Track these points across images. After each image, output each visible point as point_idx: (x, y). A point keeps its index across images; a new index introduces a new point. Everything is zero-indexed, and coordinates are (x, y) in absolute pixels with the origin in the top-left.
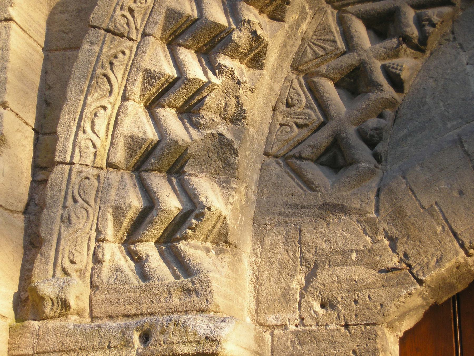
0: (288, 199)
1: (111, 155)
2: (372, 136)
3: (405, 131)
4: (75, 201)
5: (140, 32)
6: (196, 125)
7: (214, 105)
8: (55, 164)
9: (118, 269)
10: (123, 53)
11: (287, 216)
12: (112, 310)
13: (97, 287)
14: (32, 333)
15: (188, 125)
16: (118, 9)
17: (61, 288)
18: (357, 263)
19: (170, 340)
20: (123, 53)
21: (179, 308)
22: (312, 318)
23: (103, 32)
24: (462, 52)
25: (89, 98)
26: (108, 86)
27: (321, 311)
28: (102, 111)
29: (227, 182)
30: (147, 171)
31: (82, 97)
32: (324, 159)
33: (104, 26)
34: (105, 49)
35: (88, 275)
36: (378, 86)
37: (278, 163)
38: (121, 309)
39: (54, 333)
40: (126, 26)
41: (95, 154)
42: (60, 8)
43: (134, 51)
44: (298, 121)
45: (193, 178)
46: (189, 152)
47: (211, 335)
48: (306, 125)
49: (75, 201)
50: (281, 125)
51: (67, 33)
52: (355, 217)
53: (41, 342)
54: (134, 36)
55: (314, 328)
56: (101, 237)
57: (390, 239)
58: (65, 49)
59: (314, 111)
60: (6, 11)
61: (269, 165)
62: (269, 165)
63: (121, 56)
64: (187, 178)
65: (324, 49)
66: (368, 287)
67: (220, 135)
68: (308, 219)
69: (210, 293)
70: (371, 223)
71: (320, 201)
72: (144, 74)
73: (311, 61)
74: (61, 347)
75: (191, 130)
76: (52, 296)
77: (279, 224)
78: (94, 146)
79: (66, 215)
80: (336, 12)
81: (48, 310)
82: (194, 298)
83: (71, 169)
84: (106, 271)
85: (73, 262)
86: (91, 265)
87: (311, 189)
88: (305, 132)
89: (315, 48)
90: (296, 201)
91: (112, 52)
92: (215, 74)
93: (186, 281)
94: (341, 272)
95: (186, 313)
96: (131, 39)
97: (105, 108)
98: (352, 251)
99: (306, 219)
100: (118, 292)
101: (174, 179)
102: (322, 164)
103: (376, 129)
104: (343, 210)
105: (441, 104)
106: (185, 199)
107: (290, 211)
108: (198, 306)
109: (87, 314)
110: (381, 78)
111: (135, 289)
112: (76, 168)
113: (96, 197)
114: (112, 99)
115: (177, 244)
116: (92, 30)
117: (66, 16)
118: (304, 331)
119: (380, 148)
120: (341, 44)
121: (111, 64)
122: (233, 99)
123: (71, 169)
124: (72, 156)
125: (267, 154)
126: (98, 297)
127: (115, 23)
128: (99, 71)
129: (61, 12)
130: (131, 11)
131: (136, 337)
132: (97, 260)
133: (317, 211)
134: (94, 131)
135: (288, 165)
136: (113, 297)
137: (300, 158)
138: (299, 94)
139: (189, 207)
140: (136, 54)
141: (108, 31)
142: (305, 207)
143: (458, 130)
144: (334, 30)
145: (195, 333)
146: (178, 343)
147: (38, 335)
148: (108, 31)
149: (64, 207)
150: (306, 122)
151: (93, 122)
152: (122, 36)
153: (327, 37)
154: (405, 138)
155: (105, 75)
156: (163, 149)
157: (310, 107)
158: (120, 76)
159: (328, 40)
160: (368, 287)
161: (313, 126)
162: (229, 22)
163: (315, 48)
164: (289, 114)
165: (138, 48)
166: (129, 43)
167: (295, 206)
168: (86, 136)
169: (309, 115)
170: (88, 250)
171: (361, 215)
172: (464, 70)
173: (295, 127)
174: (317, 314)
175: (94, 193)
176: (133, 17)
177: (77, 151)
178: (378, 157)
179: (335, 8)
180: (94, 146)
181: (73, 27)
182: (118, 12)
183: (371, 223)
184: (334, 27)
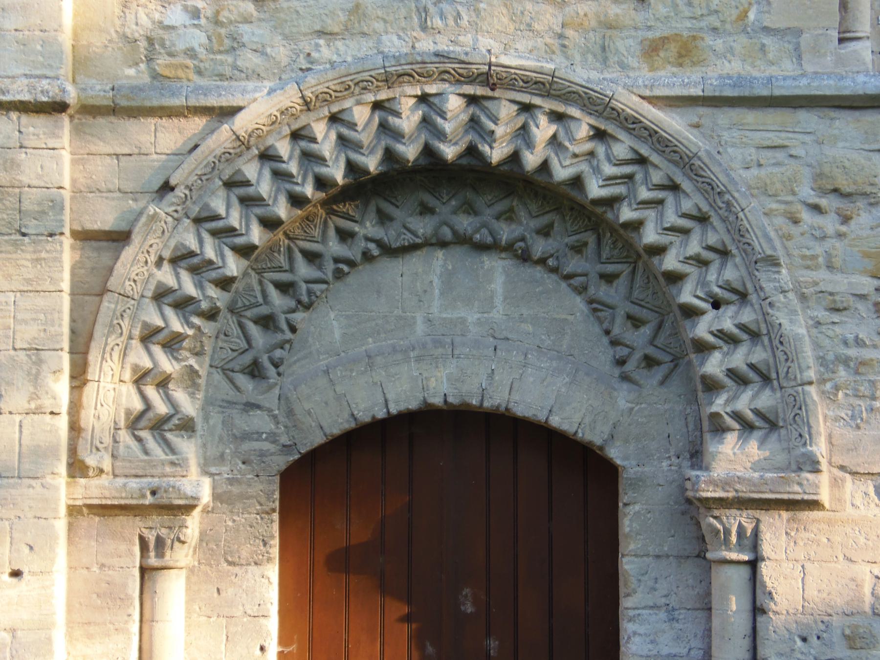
0: (225, 397)
1: (122, 375)
2: (277, 363)
3: (296, 358)
4: (102, 405)
5: (140, 294)
6: (176, 359)
7: (187, 347)
8: (88, 381)
9: (128, 447)
10: (129, 308)
11: (224, 407)
12: (127, 472)
13: (117, 457)
14: (81, 486)
15: (170, 358)
16: (127, 280)
17: (99, 461)
18: (266, 439)
19: (170, 496)
20: (129, 308)
21: (170, 474)
22: (238, 470)
23: (117, 295)
24: (331, 312)
25: (109, 339)
26: (120, 331)
27: (243, 467)
28: (116, 347)
29: (194, 393)
30: (144, 385)
31: (104, 338)
32: (246, 371)
33: (118, 291)
34: (119, 307)
35: (110, 450)
36: (282, 331)
37: (218, 373)
38: (133, 472)
39: (96, 487)
40: (131, 292)
41: (113, 375)
42: (79, 265)
43: (136, 306)
44: (232, 347)
45: (174, 392)
46: (172, 376)
47: (194, 495)
48: (237, 350)
49: (102, 405)
50: (221, 348)
51: (85, 284)
52: (265, 413)
53: (88, 492)
54: (136, 297)
55: (239, 476)
56: (118, 427)
57: (286, 427)
58: (84, 295)
59: (242, 341)
60: (59, 286)
61: (212, 373)
62: (212, 373)
63: (128, 311)
64: (170, 392)
65: (249, 301)
66: (272, 454)
67: (191, 366)
68: (237, 411)
69: (189, 467)
70: (275, 417)
71: (244, 401)
72: (142, 326)
73: (241, 308)
74: (101, 496)
75: (173, 361)
76: (94, 466)
77: (219, 412)
78: (112, 370)
79: (97, 414)
80: (257, 275)
81: (91, 473)
82: (179, 469)
83: (99, 385)
84: (122, 449)
85: (101, 443)
86: (111, 444)
87: (239, 391)
88: (236, 354)
89: (244, 299)
90: (229, 398)
91: (123, 309)
92: (189, 327)
93: (172, 457)
94: (256, 445)
95: (174, 477)
96: (133, 299)
97: (118, 345)
98: (263, 433)
99: (235, 411)
100: (130, 461)
101: (161, 391)
102: (244, 373)
103: (280, 358)
104: (258, 407)
105: (317, 343)
106: (170, 406)
107: (225, 405)
108: (181, 474)
109: (111, 474)
110: (284, 327)
111: (142, 461)
112: (102, 384)
113: (114, 401)
114: (122, 339)
115: (165, 434)
116: (110, 293)
117: (83, 271)
118: (233, 478)
119: (281, 369)
120: (260, 300)
121: (122, 316)
122: (199, 343)
123: (99, 385)
124: (100, 377)
125: (211, 366)
126: (118, 464)
127: (125, 289)
128: (115, 322)
129: (80, 268)
130: (135, 281)
131: (148, 493)
132: (116, 441)
133: (242, 407)
134: (112, 360)
135: (224, 374)
136: (128, 465)
137: (233, 371)
138: (232, 330)
139: (172, 412)
140: (137, 309)
141: (120, 294)
142: (235, 403)
143: (326, 361)
144: (255, 289)
145: (185, 494)
146: (175, 498)
147: (86, 487)
148: (120, 294)
149: (96, 409)
150: (237, 348)
151: (111, 354)
152: (128, 297)
153: (251, 293)
154: (295, 362)
155: (119, 324)
156: (156, 374)
157: (238, 338)
158: (127, 323)
159: (252, 295)
160: (272, 454)
161: (240, 351)
162: (198, 295)
163: (244, 299)
164: (226, 341)
165: (138, 304)
166: (133, 302)
167: (228, 402)
168: (107, 364)
169: (239, 344)
170: (110, 434)
171: (269, 412)
172: (332, 324)
173: (229, 350)
174: (240, 468)
175: (112, 399)
176: (136, 285)
177: (102, 373)
178: (279, 374)
179: (257, 273)
180: (112, 370)
181: (89, 280)
182: (127, 283)
183: (275, 417)
184: (257, 288)
